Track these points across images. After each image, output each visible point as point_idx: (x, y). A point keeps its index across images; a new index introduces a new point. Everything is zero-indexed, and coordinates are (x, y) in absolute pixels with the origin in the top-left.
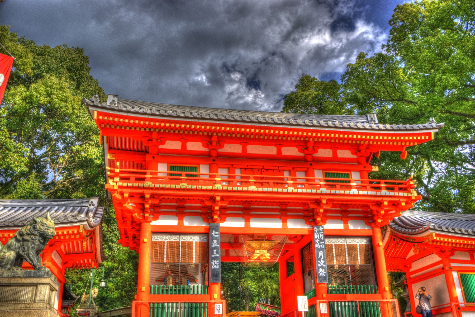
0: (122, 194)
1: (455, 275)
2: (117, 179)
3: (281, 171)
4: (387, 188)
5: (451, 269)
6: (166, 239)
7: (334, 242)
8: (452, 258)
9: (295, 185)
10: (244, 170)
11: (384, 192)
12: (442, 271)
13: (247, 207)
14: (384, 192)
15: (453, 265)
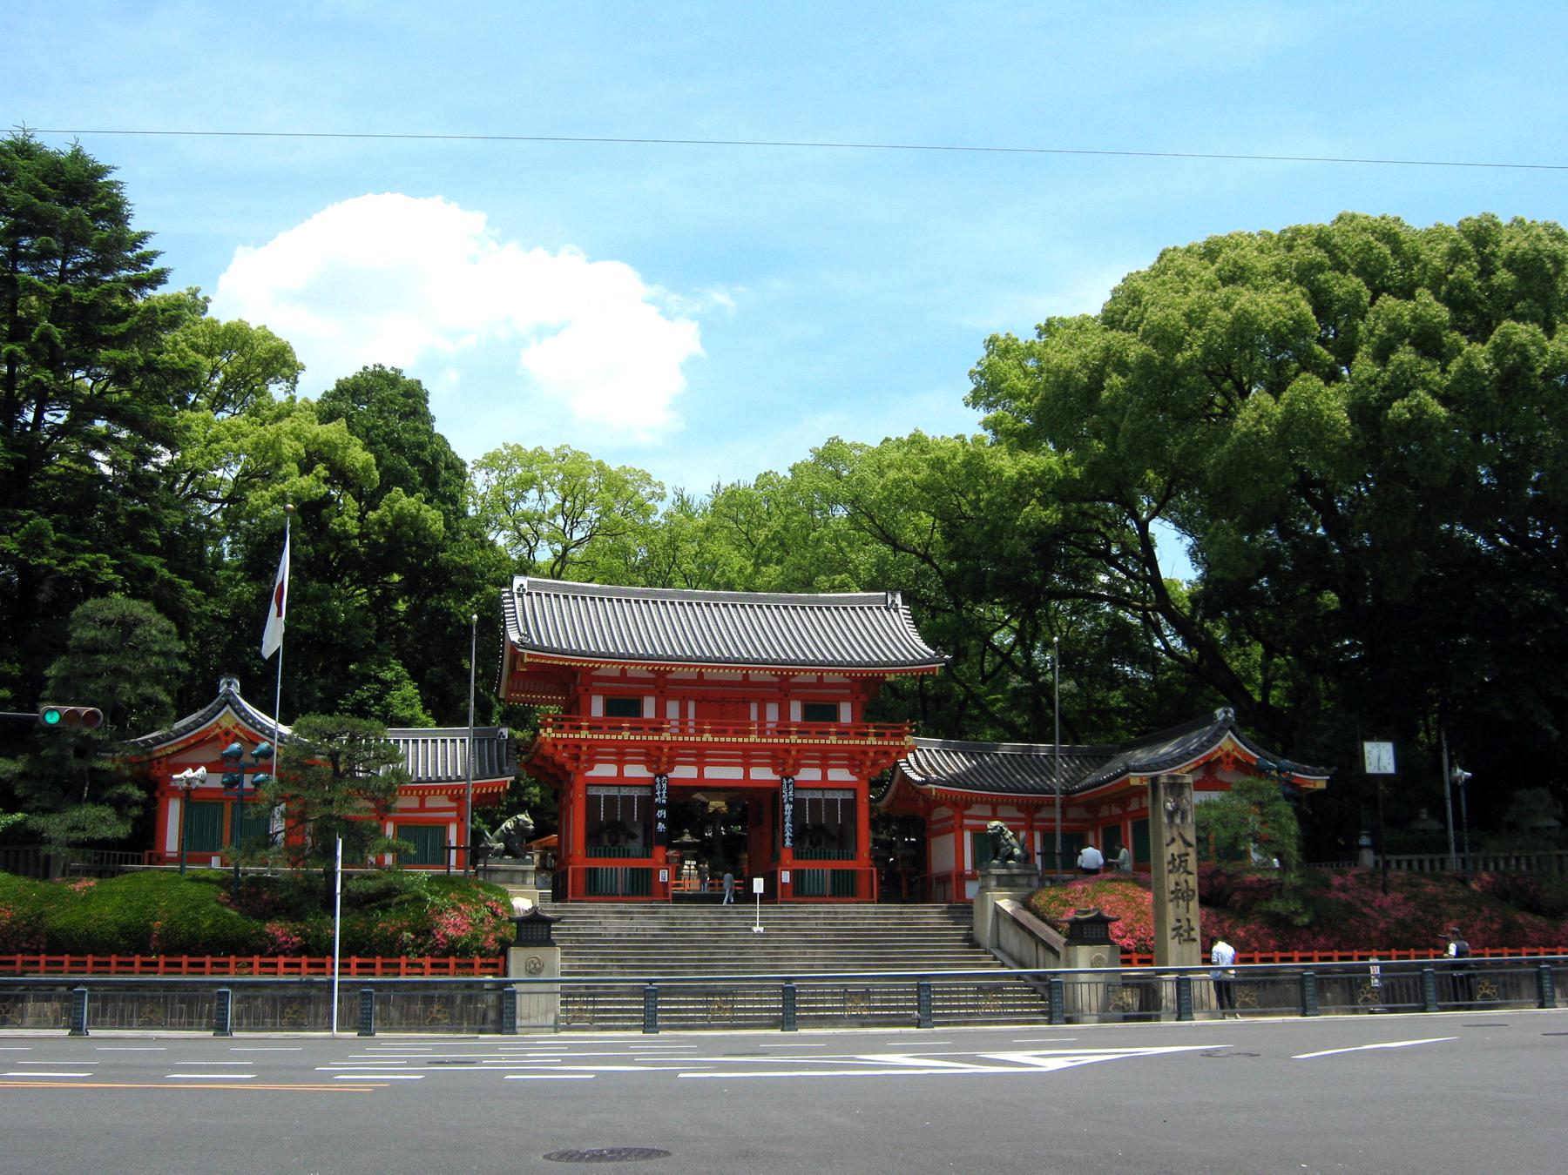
0: (555, 746)
1: (967, 835)
2: (549, 730)
3: (746, 702)
4: (875, 735)
5: (962, 827)
6: (603, 792)
7: (808, 795)
8: (967, 812)
9: (761, 733)
10: (698, 702)
11: (872, 741)
12: (951, 830)
13: (701, 756)
14: (872, 741)
15: (966, 822)
